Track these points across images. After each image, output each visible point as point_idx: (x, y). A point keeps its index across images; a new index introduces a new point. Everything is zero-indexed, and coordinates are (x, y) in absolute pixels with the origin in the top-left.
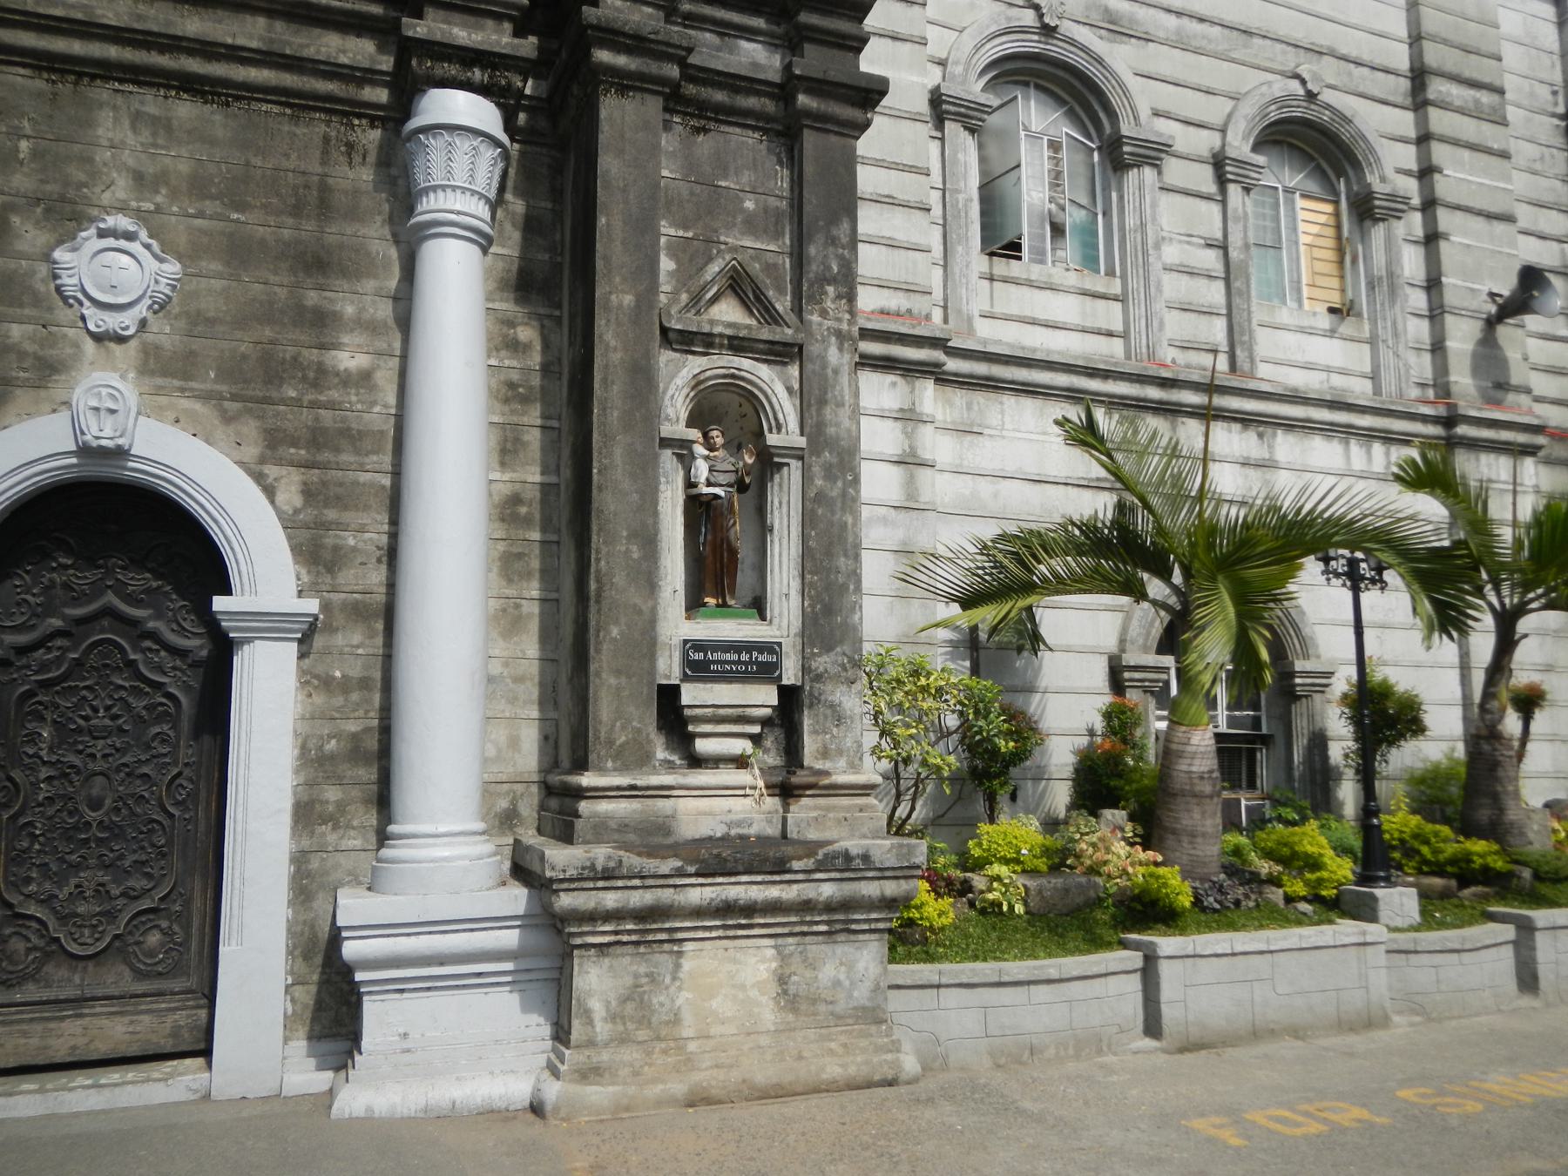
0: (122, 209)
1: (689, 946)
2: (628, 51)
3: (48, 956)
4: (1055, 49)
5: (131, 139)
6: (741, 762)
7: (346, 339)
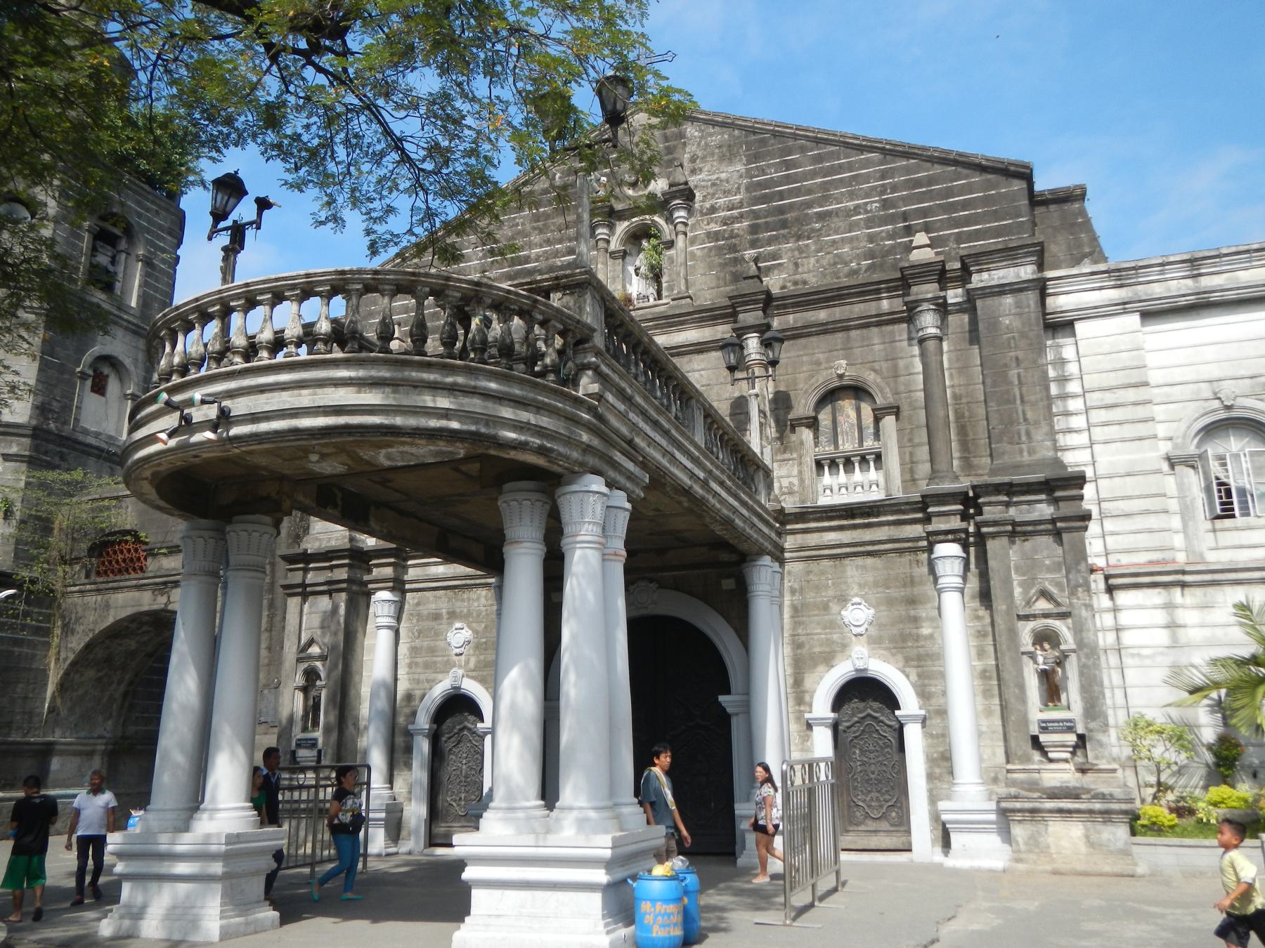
0: (857, 595)
1: (1050, 823)
2: (992, 526)
3: (866, 817)
4: (1234, 414)
5: (856, 573)
6: (1066, 761)
7: (924, 624)
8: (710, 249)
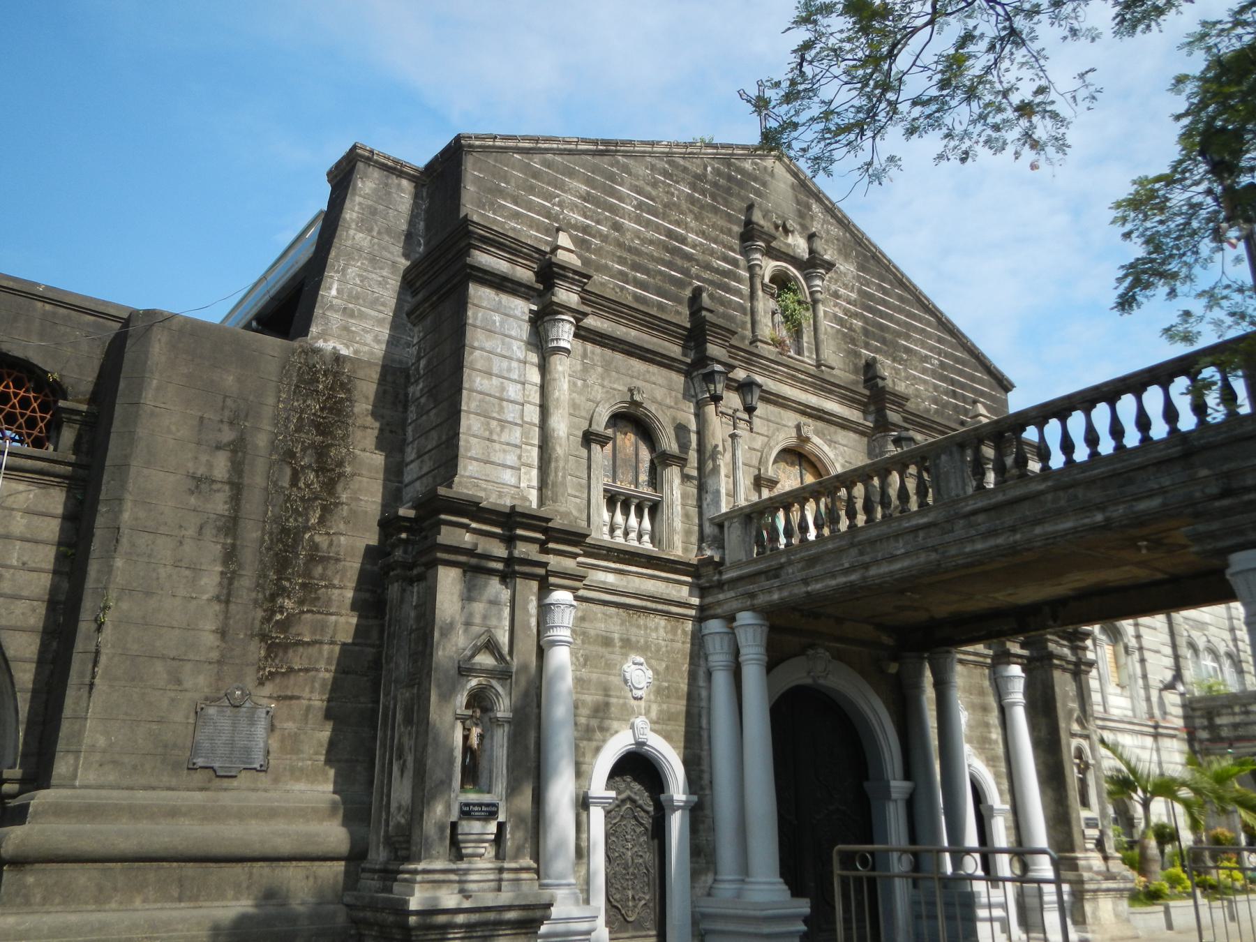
8: (838, 331)
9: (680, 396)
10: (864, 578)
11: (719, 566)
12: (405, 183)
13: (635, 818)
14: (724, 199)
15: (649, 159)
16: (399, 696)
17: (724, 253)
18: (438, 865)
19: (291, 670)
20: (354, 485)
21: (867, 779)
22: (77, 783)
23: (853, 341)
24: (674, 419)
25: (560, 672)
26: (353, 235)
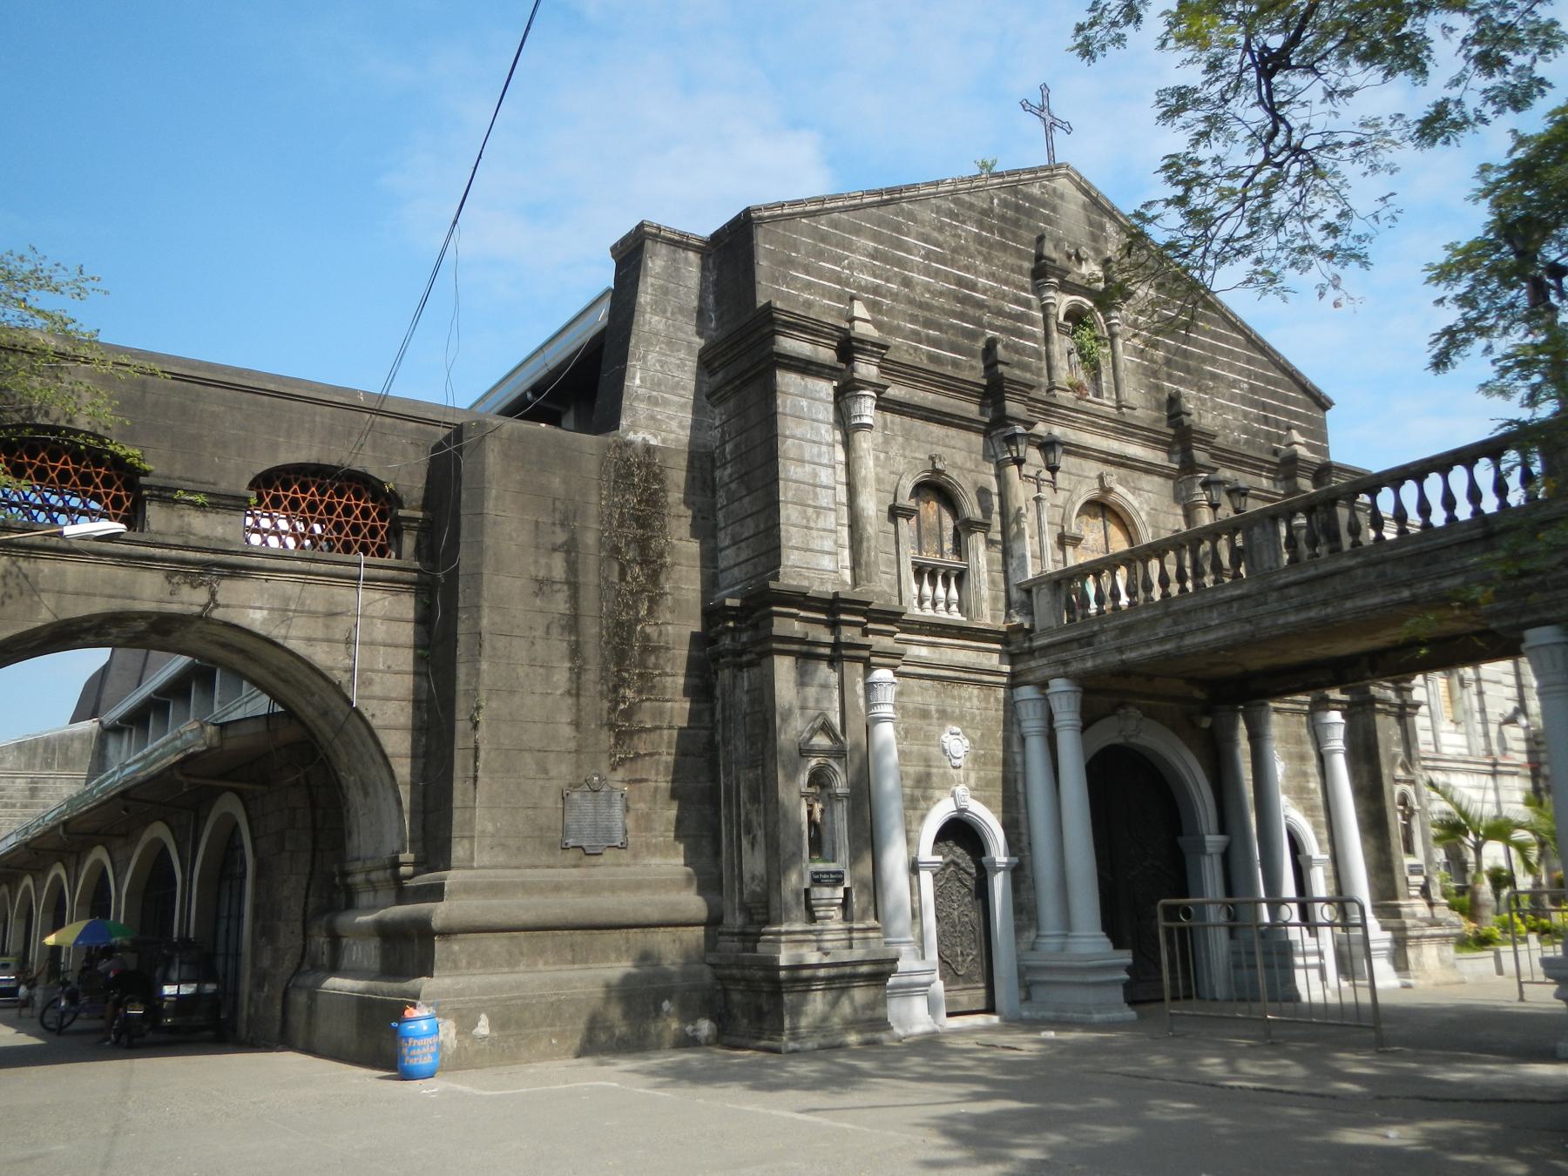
8: (1139, 364)
9: (980, 458)
10: (1179, 648)
11: (1029, 633)
12: (691, 255)
13: (960, 880)
14: (1013, 233)
15: (933, 201)
16: (742, 777)
17: (1015, 295)
18: (798, 927)
19: (638, 755)
20: (675, 576)
21: (1181, 834)
22: (475, 865)
23: (1155, 374)
24: (975, 483)
25: (886, 745)
26: (650, 320)
